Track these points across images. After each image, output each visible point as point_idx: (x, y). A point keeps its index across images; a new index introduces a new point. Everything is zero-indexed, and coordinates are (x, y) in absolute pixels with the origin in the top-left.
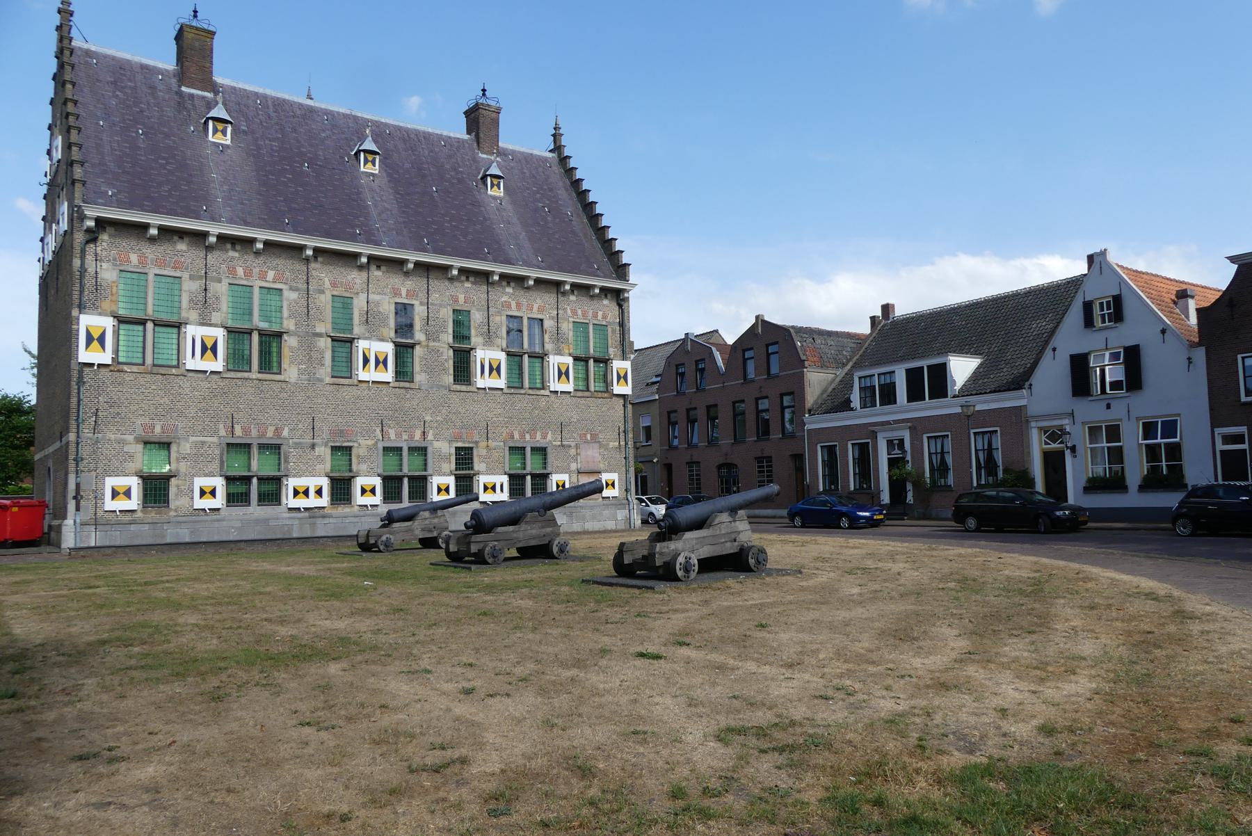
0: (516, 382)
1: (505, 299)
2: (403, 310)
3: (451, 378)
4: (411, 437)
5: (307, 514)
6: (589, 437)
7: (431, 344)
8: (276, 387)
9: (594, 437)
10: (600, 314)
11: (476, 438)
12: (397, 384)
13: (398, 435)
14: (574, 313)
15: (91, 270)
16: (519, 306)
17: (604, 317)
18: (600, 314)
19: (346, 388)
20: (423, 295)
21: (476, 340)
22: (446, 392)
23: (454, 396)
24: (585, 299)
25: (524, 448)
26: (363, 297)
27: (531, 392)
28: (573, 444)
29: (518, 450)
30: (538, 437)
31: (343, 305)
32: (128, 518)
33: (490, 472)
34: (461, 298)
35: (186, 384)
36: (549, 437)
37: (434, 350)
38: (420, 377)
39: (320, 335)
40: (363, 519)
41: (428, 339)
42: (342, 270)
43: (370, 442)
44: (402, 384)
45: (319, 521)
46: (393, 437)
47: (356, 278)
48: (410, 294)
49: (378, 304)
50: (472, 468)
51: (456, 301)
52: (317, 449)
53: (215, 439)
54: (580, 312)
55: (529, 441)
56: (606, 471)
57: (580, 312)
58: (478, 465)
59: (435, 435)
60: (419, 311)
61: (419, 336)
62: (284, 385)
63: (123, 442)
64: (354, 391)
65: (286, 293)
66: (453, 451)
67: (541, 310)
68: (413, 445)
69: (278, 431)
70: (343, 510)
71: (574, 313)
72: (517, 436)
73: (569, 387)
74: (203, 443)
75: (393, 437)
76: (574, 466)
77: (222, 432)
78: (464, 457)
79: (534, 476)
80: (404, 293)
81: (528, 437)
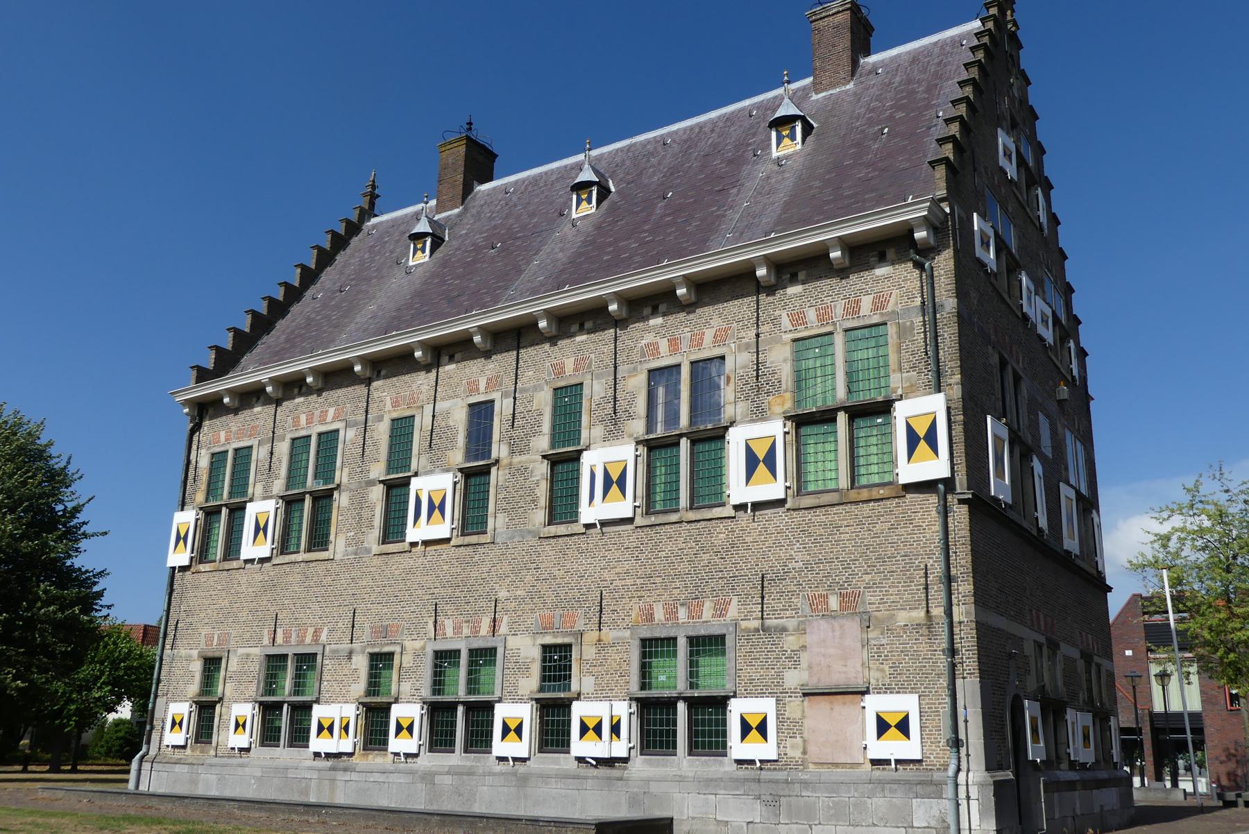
0: (656, 500)
1: (649, 338)
2: (481, 414)
3: (540, 516)
4: (475, 631)
5: (329, 763)
6: (834, 602)
7: (517, 459)
8: (321, 567)
9: (850, 602)
10: (866, 303)
11: (580, 626)
12: (460, 541)
13: (457, 629)
14: (799, 319)
15: (193, 462)
16: (674, 345)
17: (878, 305)
18: (866, 303)
19: (396, 558)
20: (508, 382)
21: (590, 430)
22: (534, 541)
23: (548, 548)
24: (825, 284)
25: (675, 639)
26: (428, 409)
27: (692, 515)
28: (791, 624)
29: (654, 648)
30: (707, 613)
31: (402, 429)
32: (179, 754)
33: (602, 694)
34: (569, 364)
35: (242, 577)
36: (733, 612)
37: (522, 465)
38: (497, 522)
39: (371, 483)
40: (393, 778)
41: (512, 453)
42: (406, 378)
43: (418, 644)
44: (468, 539)
45: (341, 776)
46: (449, 632)
47: (422, 382)
48: (492, 384)
49: (448, 413)
50: (568, 688)
51: (559, 371)
52: (354, 658)
53: (256, 651)
54: (811, 315)
55: (684, 625)
56: (888, 690)
57: (811, 315)
58: (580, 680)
59: (511, 625)
60: (503, 407)
61: (499, 450)
62: (328, 564)
63: (189, 659)
64: (406, 561)
65: (342, 433)
66: (536, 653)
67: (719, 340)
68: (477, 644)
69: (317, 633)
70: (376, 760)
71: (799, 319)
72: (659, 615)
73: (773, 489)
74: (248, 655)
75: (449, 632)
76: (793, 679)
77: (266, 641)
78: (556, 664)
79: (693, 703)
80: (482, 386)
81: (682, 613)
